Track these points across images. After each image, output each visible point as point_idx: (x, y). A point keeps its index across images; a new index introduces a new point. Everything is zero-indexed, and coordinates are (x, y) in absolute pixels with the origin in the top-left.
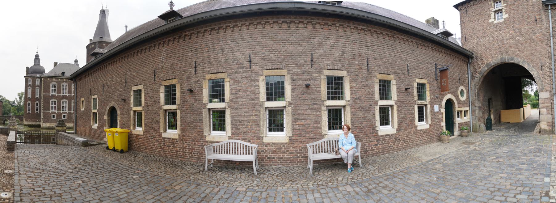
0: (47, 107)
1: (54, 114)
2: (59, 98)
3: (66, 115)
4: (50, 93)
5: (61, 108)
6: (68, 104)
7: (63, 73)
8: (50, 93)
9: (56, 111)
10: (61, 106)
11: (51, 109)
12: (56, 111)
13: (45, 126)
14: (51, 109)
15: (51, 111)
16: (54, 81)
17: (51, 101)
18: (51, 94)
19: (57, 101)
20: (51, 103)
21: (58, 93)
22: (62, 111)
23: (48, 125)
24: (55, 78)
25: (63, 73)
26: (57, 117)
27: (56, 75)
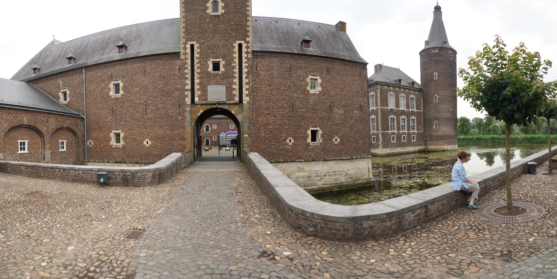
0: (385, 127)
1: (393, 136)
2: (399, 113)
3: (405, 136)
4: (388, 107)
5: (400, 127)
6: (407, 122)
7: (400, 80)
8: (388, 107)
9: (395, 131)
10: (400, 124)
11: (390, 129)
12: (395, 131)
13: (385, 153)
14: (390, 129)
15: (390, 132)
16: (392, 91)
17: (390, 117)
18: (389, 108)
19: (396, 118)
20: (390, 120)
21: (396, 108)
22: (401, 131)
23: (388, 151)
24: (392, 86)
25: (400, 80)
26: (397, 140)
27: (391, 82)
